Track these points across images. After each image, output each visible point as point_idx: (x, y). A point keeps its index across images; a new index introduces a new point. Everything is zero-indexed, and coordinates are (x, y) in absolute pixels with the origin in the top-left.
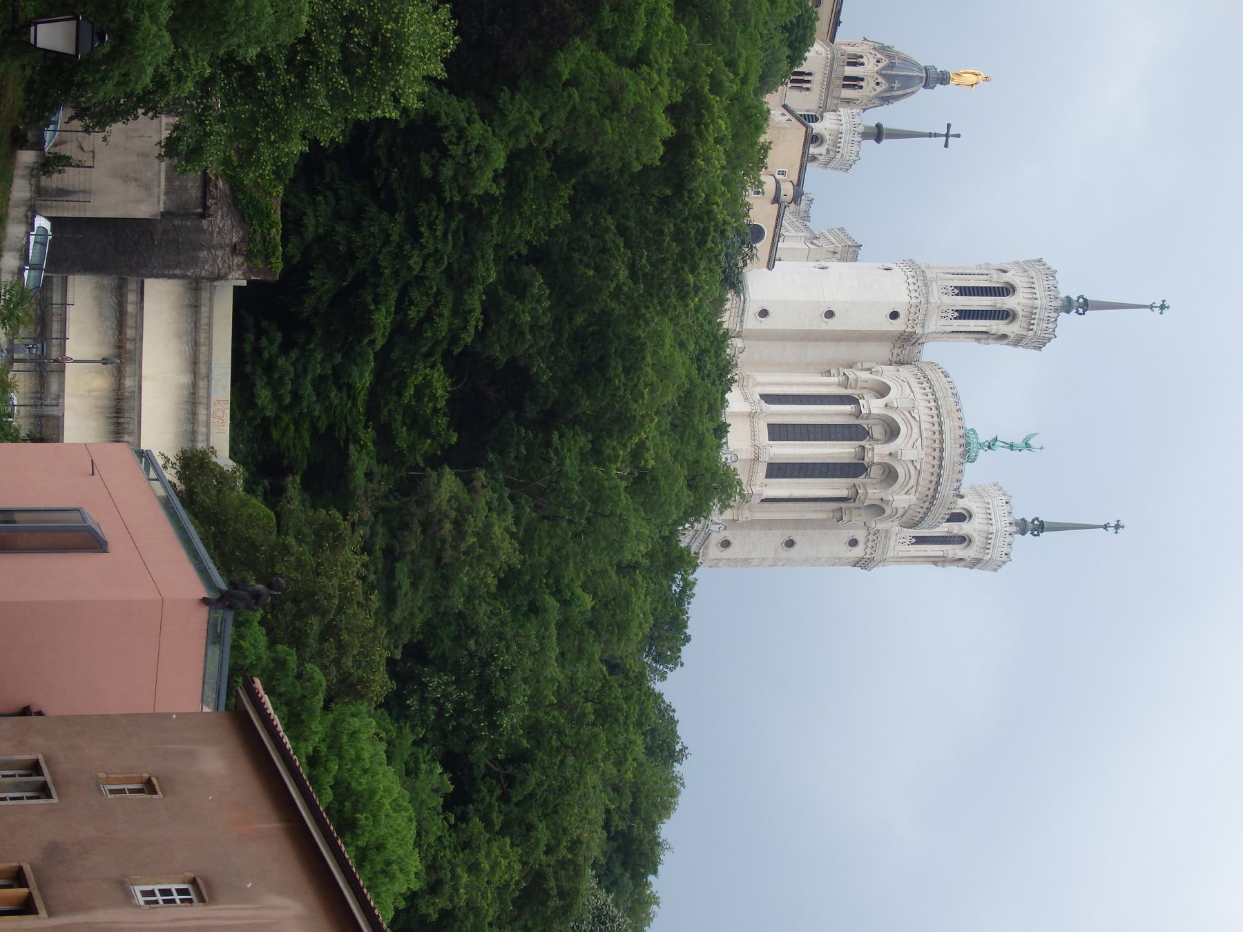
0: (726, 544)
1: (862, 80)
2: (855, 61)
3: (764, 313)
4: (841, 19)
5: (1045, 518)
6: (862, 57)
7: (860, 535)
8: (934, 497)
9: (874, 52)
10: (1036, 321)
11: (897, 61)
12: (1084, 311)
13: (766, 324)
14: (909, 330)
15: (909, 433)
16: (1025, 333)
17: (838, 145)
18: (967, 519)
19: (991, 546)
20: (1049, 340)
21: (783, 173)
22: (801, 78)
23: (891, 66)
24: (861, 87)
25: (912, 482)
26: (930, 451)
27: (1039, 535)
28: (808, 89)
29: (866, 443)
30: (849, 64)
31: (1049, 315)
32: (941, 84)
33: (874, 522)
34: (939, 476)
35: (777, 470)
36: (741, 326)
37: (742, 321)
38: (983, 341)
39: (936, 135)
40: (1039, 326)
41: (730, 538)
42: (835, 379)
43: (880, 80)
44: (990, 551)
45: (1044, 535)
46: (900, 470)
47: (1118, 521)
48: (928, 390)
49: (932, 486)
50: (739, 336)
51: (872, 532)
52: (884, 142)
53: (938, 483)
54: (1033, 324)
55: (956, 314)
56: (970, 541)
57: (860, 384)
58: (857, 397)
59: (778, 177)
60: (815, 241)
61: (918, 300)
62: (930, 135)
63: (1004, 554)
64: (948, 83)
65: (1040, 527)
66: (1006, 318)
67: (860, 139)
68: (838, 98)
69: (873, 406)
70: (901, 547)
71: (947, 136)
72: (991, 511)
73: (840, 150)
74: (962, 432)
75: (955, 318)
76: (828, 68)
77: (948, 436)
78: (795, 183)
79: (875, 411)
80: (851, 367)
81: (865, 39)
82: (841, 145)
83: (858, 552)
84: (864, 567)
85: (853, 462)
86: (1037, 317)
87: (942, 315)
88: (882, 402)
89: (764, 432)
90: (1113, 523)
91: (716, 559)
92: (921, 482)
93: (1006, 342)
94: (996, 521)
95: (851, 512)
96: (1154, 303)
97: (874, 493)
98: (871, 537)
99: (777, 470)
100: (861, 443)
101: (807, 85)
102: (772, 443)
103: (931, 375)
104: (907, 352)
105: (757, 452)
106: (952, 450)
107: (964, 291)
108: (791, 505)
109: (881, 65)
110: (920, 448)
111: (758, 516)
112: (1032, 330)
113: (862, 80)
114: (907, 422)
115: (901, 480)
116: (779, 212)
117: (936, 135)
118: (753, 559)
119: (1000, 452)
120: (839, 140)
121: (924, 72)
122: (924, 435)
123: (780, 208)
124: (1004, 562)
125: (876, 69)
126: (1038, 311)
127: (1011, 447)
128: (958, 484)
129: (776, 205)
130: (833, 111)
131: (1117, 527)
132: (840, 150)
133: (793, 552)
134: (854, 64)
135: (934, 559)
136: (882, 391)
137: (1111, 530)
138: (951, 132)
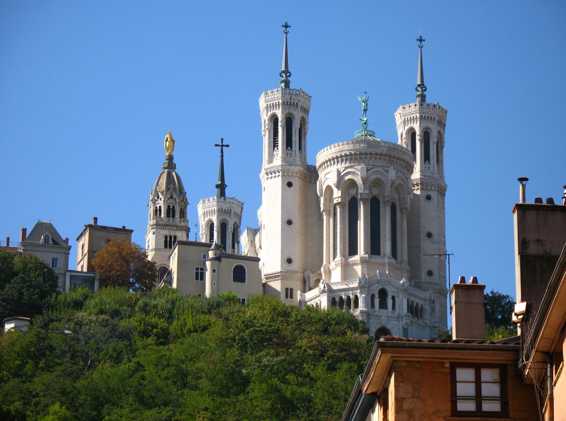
0: (430, 273)
1: (169, 206)
3: (289, 261)
4: (120, 227)
6: (156, 207)
10: (292, 101)
16: (299, 107)
17: (226, 210)
24: (174, 207)
25: (380, 169)
27: (426, 87)
30: (160, 215)
34: (376, 154)
39: (222, 152)
41: (426, 271)
44: (433, 116)
46: (373, 177)
49: (383, 157)
53: (381, 155)
55: (289, 148)
56: (427, 128)
62: (222, 156)
66: (291, 119)
69: (337, 194)
70: (431, 169)
71: (222, 146)
75: (291, 148)
85: (369, 205)
86: (289, 101)
88: (335, 190)
92: (380, 164)
93: (306, 117)
96: (284, 31)
101: (173, 238)
105: (363, 262)
107: (275, 144)
111: (406, 258)
112: (297, 103)
115: (379, 176)
116: (226, 257)
117: (222, 152)
121: (165, 170)
129: (222, 259)
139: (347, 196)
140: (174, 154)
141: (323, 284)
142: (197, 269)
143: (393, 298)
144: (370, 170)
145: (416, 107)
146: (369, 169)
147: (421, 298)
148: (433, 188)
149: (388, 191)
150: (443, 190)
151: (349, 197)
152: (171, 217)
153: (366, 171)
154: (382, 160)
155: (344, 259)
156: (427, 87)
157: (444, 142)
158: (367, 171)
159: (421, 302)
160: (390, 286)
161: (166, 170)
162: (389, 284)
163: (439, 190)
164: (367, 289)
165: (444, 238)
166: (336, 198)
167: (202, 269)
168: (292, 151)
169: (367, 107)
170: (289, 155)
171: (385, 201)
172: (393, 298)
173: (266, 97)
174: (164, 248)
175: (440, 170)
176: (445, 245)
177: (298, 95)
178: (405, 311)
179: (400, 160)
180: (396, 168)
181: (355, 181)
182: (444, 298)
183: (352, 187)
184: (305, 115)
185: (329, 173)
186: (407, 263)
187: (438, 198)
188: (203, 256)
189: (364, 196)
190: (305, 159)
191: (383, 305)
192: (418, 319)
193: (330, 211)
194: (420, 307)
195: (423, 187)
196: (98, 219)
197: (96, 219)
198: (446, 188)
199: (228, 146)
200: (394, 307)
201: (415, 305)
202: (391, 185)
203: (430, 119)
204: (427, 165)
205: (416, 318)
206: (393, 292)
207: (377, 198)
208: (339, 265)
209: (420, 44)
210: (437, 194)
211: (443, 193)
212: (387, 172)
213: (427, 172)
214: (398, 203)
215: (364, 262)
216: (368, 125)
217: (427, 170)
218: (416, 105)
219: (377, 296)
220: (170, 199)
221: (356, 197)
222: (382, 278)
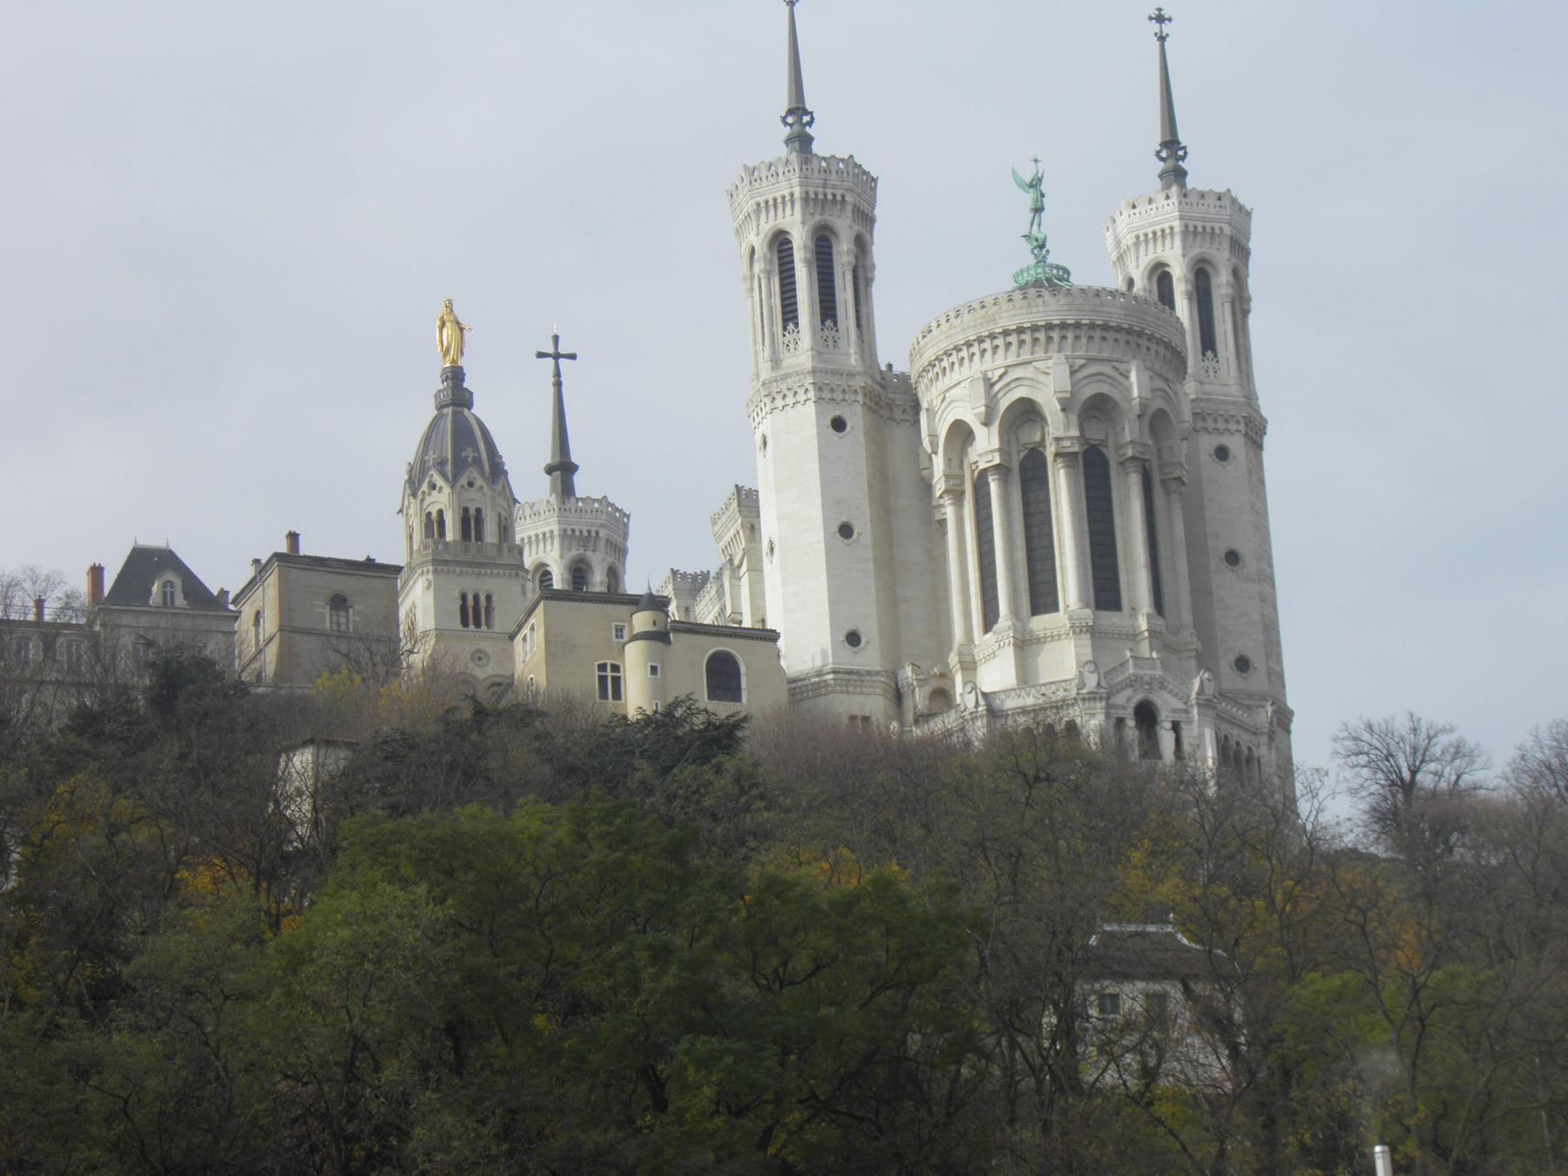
0: (1242, 664)
1: (466, 510)
2: (434, 525)
4: (361, 558)
5: (1155, 137)
6: (429, 514)
7: (1207, 443)
8: (1130, 331)
9: (420, 496)
11: (431, 457)
12: (806, 112)
13: (870, 632)
14: (860, 398)
15: (1027, 382)
16: (849, 208)
17: (585, 534)
18: (1167, 269)
19: (1208, 225)
20: (859, 166)
22: (470, 610)
23: (441, 465)
24: (479, 511)
25: (1107, 369)
26: (1054, 347)
27: (1184, 148)
29: (1050, 451)
30: (442, 533)
31: (816, 171)
32: (463, 380)
33: (1181, 425)
36: (877, 673)
37: (869, 673)
38: (869, 275)
39: (558, 374)
41: (1232, 657)
42: (949, 512)
43: (464, 481)
44: (1216, 225)
45: (1183, 138)
46: (1089, 391)
47: (1151, 18)
48: (954, 358)
49: (1111, 336)
50: (894, 676)
51: (1200, 424)
52: (575, 458)
53: (1106, 327)
54: (834, 195)
55: (829, 323)
58: (976, 472)
59: (626, 637)
60: (736, 562)
61: (811, 388)
62: (558, 384)
63: (1218, 203)
64: (461, 368)
65: (1172, 145)
66: (828, 240)
67: (572, 499)
68: (499, 547)
69: (986, 447)
71: (557, 356)
72: (1149, 231)
73: (593, 530)
74: (1018, 295)
75: (835, 324)
76: (452, 569)
78: (633, 608)
79: (995, 443)
80: (927, 487)
81: (401, 511)
82: (585, 529)
83: (1236, 444)
84: (1261, 431)
85: (1082, 470)
87: (831, 346)
88: (979, 431)
90: (1155, 27)
91: (1269, 679)
92: (1105, 355)
94: (1166, 221)
97: (1130, 431)
98: (1210, 424)
100: (1050, 458)
102: (1061, 606)
103: (929, 355)
104: (897, 397)
105: (1078, 630)
107: (789, 314)
108: (1164, 564)
109: (439, 481)
110: (1050, 363)
111: (1187, 617)
112: (843, 197)
113: (466, 510)
115: (1104, 388)
117: (558, 374)
118: (1263, 616)
119: (1050, 225)
120: (577, 533)
122: (1026, 356)
124: (1234, 201)
125: (447, 490)
126: (811, 191)
127: (1038, 210)
128: (1103, 294)
130: (521, 552)
131: (1160, 19)
132: (593, 530)
133: (1245, 551)
134: (441, 523)
135: (1239, 317)
136: (961, 434)
137: (1166, 28)
138: (551, 350)
139: (1014, 449)
141: (973, 694)
142: (602, 667)
143: (1176, 727)
144: (1077, 371)
145: (1170, 201)
146: (1076, 368)
149: (1130, 431)
150: (1256, 433)
152: (473, 540)
153: (1068, 373)
154: (1111, 343)
156: (1188, 150)
157: (1248, 300)
158: (1072, 373)
159: (1245, 738)
160: (1164, 694)
161: (449, 410)
162: (1161, 688)
163: (1249, 432)
164: (1104, 703)
166: (986, 453)
167: (615, 668)
168: (837, 331)
169: (1042, 201)
170: (830, 343)
171: (1125, 457)
172: (1176, 727)
173: (754, 183)
174: (460, 627)
176: (1273, 586)
177: (845, 174)
179: (1158, 343)
180: (1148, 364)
181: (1038, 404)
182: (1285, 733)
183: (1025, 422)
184: (864, 232)
185: (959, 383)
186: (1194, 631)
187: (1247, 455)
188: (617, 630)
189: (1067, 443)
190: (873, 355)
193: (963, 493)
195: (1206, 425)
196: (301, 539)
197: (293, 537)
198: (1265, 428)
199: (573, 357)
202: (1139, 413)
204: (1212, 364)
206: (1174, 711)
207: (1102, 452)
208: (1007, 641)
209: (1158, 31)
210: (1246, 444)
211: (1258, 440)
213: (1211, 383)
214: (1155, 465)
215: (1081, 631)
216: (1048, 251)
217: (1212, 378)
218: (1168, 197)
219: (1131, 723)
220: (466, 490)
221: (1041, 449)
222: (1141, 672)
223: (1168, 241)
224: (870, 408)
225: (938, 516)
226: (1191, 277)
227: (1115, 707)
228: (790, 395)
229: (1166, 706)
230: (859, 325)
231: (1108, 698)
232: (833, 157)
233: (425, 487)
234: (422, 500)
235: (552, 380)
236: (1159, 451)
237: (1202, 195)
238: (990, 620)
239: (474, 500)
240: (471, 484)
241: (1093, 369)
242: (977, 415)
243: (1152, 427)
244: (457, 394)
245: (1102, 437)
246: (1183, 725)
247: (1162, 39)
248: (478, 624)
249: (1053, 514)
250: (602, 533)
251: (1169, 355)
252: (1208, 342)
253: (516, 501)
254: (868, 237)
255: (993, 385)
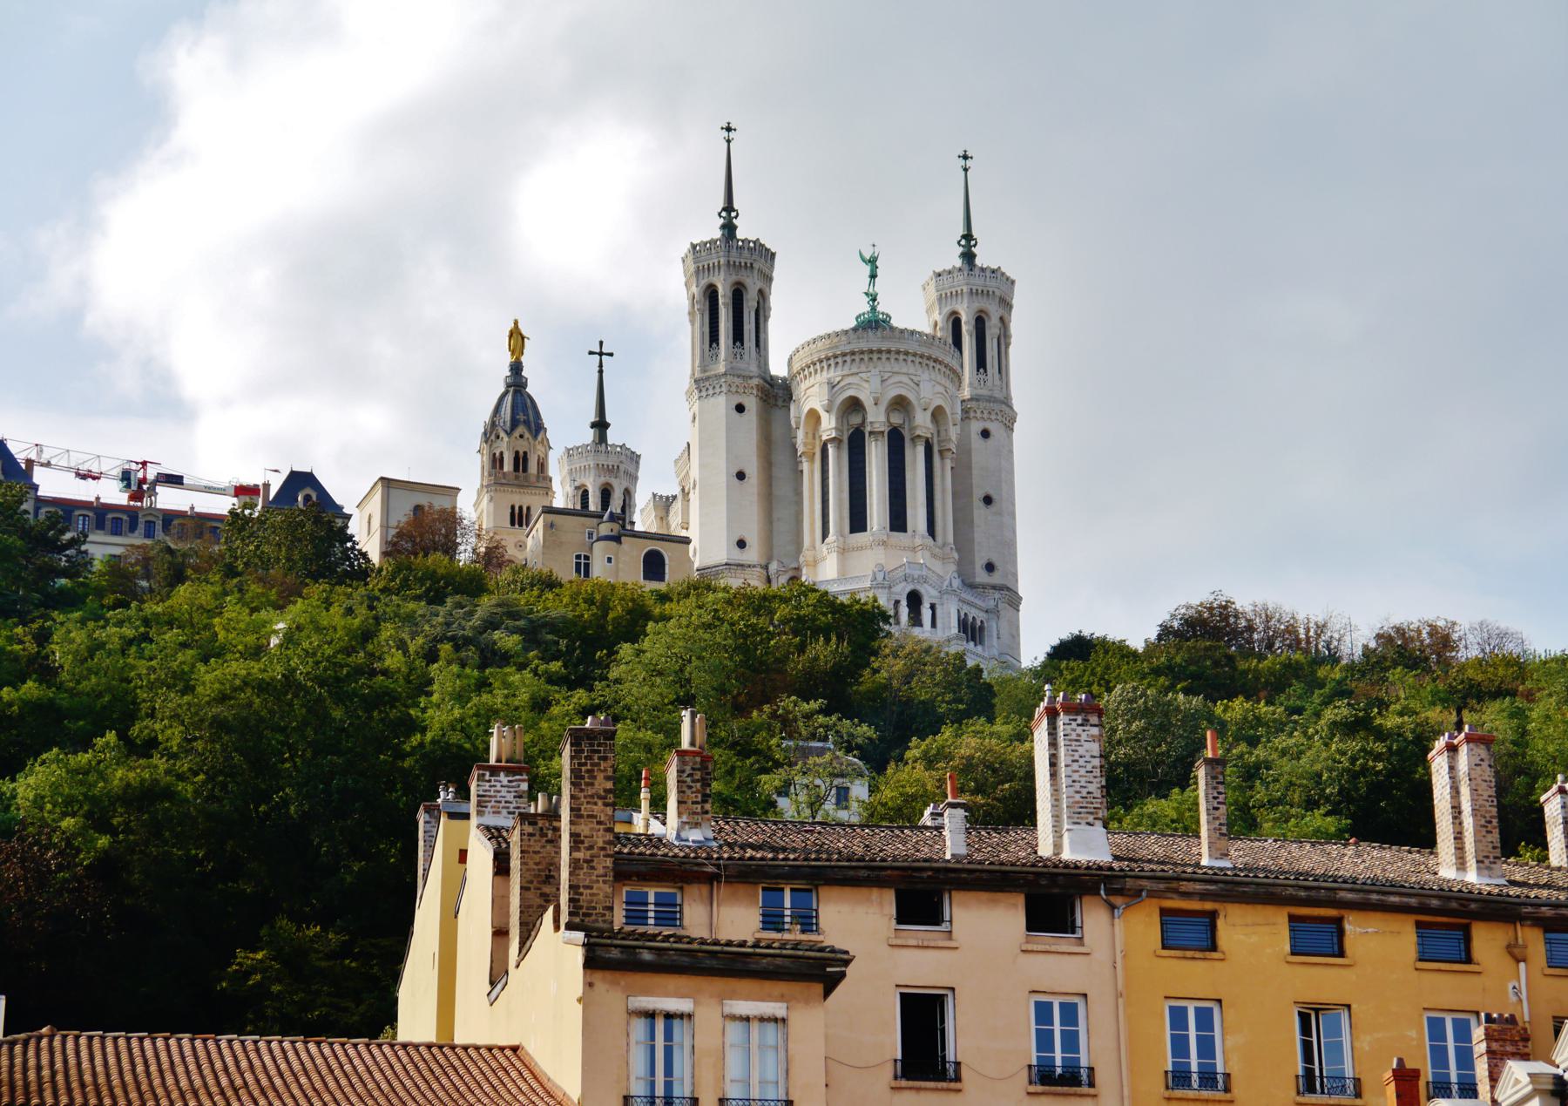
1: (517, 453)
2: (497, 461)
3: (741, 544)
7: (976, 427)
9: (490, 442)
12: (734, 210)
14: (755, 392)
20: (763, 246)
21: (591, 535)
24: (525, 453)
25: (905, 379)
28: (528, 508)
29: (868, 429)
30: (502, 467)
34: (898, 352)
35: (898, 521)
36: (754, 566)
39: (601, 365)
40: (746, 258)
41: (984, 562)
42: (805, 466)
43: (517, 433)
44: (991, 290)
45: (975, 233)
46: (893, 393)
52: (608, 420)
55: (738, 344)
56: (981, 311)
57: (810, 439)
59: (595, 538)
62: (601, 372)
64: (521, 363)
68: (538, 477)
69: (828, 425)
70: (989, 383)
71: (601, 354)
75: (742, 344)
77: (864, 346)
79: (833, 424)
82: (610, 464)
86: (737, 260)
88: (824, 416)
89: (860, 537)
90: (962, 162)
92: (905, 370)
95: (943, 441)
99: (898, 521)
100: (867, 435)
106: (873, 341)
111: (951, 539)
112: (751, 264)
114: (843, 389)
115: (903, 392)
117: (601, 365)
119: (880, 286)
122: (854, 370)
123: (625, 535)
124: (1003, 274)
125: (506, 439)
127: (873, 276)
129: (623, 539)
131: (965, 157)
136: (814, 416)
137: (969, 163)
138: (598, 350)
139: (846, 427)
140: (523, 359)
142: (578, 557)
147: (980, 609)
148: (993, 417)
151: (848, 430)
155: (840, 538)
165: (1014, 505)
167: (587, 558)
170: (738, 356)
172: (933, 607)
175: (1004, 386)
176: (1014, 518)
178: (955, 630)
189: (877, 425)
191: (916, 620)
192: (975, 645)
193: (814, 454)
194: (979, 623)
199: (611, 355)
200: (934, 624)
201: (971, 619)
203: (985, 294)
205: (972, 644)
206: (931, 597)
212: (918, 385)
219: (904, 603)
223: (960, 297)
224: (761, 398)
225: (800, 468)
226: (973, 322)
227: (896, 594)
228: (711, 388)
229: (929, 595)
230: (758, 345)
231: (890, 587)
232: (746, 239)
233: (493, 437)
234: (491, 445)
235: (598, 369)
236: (939, 432)
237: (983, 270)
238: (825, 534)
239: (522, 446)
240: (521, 436)
241: (896, 378)
242: (823, 406)
243: (934, 415)
244: (517, 381)
245: (901, 422)
246: (937, 606)
247: (966, 170)
248: (521, 525)
249: (867, 469)
250: (622, 467)
251: (948, 372)
252: (981, 363)
253: (550, 448)
254: (768, 290)
255: (833, 387)
